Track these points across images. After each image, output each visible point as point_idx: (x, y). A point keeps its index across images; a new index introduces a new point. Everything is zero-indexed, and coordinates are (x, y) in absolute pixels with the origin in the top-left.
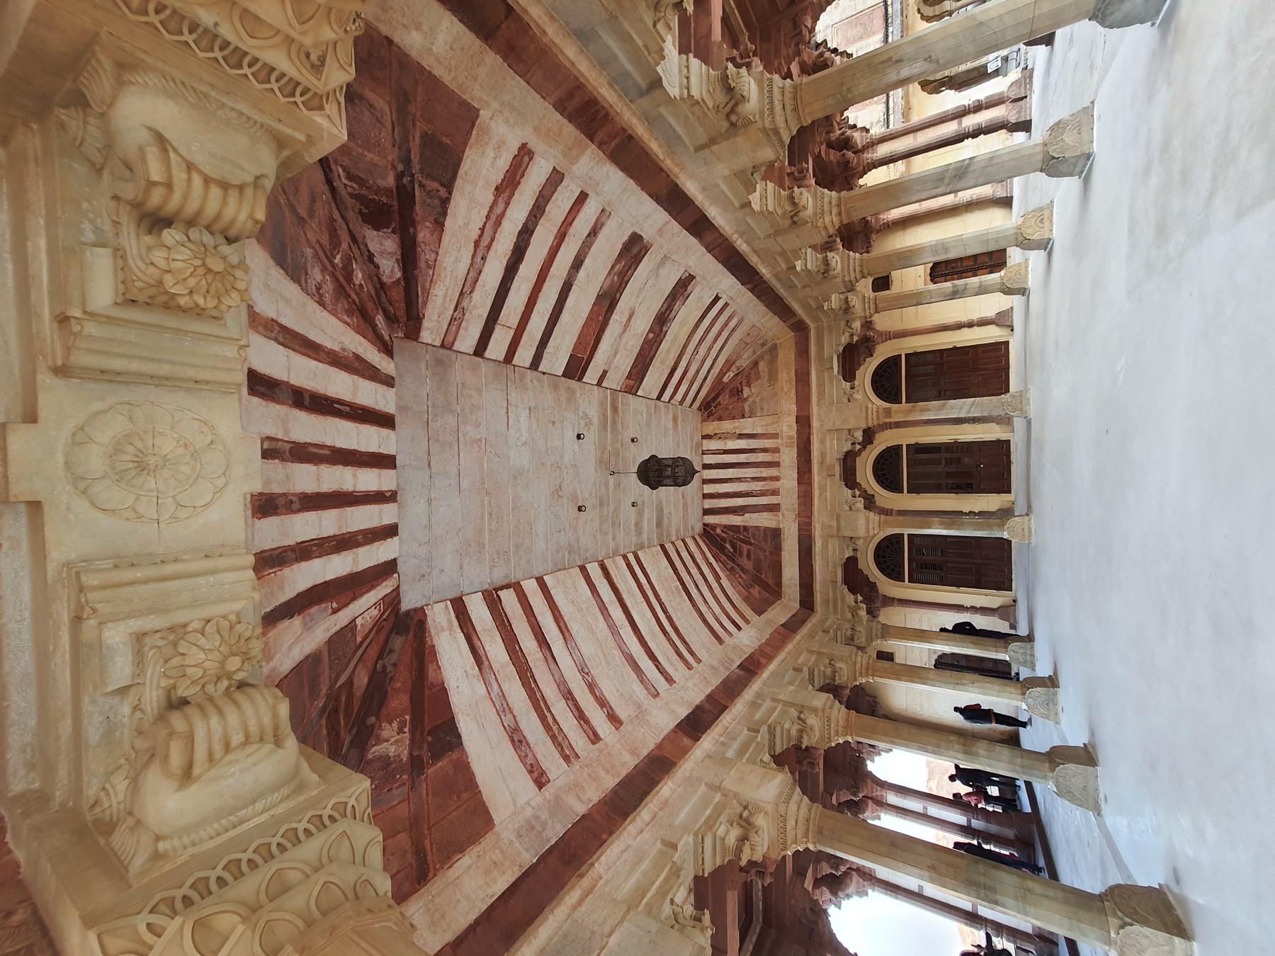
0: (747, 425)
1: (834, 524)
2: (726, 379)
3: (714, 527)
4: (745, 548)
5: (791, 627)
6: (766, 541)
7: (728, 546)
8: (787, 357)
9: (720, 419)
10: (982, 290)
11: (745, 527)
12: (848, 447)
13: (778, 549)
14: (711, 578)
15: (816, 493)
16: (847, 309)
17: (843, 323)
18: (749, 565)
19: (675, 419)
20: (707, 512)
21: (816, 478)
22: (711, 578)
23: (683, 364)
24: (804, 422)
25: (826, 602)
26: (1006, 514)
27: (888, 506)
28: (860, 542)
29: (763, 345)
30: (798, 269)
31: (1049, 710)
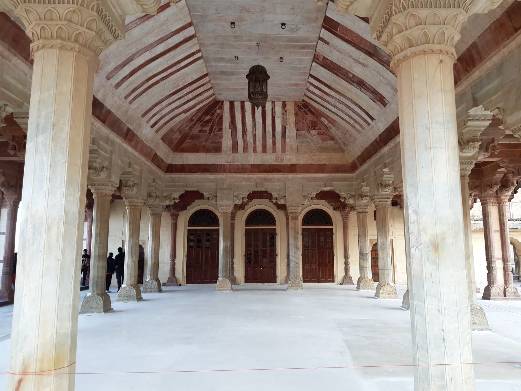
0: (291, 132)
1: (225, 186)
2: (323, 119)
3: (221, 108)
4: (207, 129)
5: (155, 159)
6: (213, 143)
7: (208, 117)
8: (336, 159)
9: (296, 114)
10: (362, 268)
11: (221, 130)
12: (275, 195)
13: (207, 150)
14: (185, 107)
15: (246, 176)
16: (361, 196)
17: (353, 193)
18: (196, 131)
19: (297, 85)
20: (232, 104)
21: (255, 176)
22: (185, 107)
23: (333, 93)
24: (292, 168)
25: (173, 181)
26: (234, 281)
27: (237, 217)
28: (213, 202)
29: (344, 144)
30: (385, 170)
31: (124, 297)
